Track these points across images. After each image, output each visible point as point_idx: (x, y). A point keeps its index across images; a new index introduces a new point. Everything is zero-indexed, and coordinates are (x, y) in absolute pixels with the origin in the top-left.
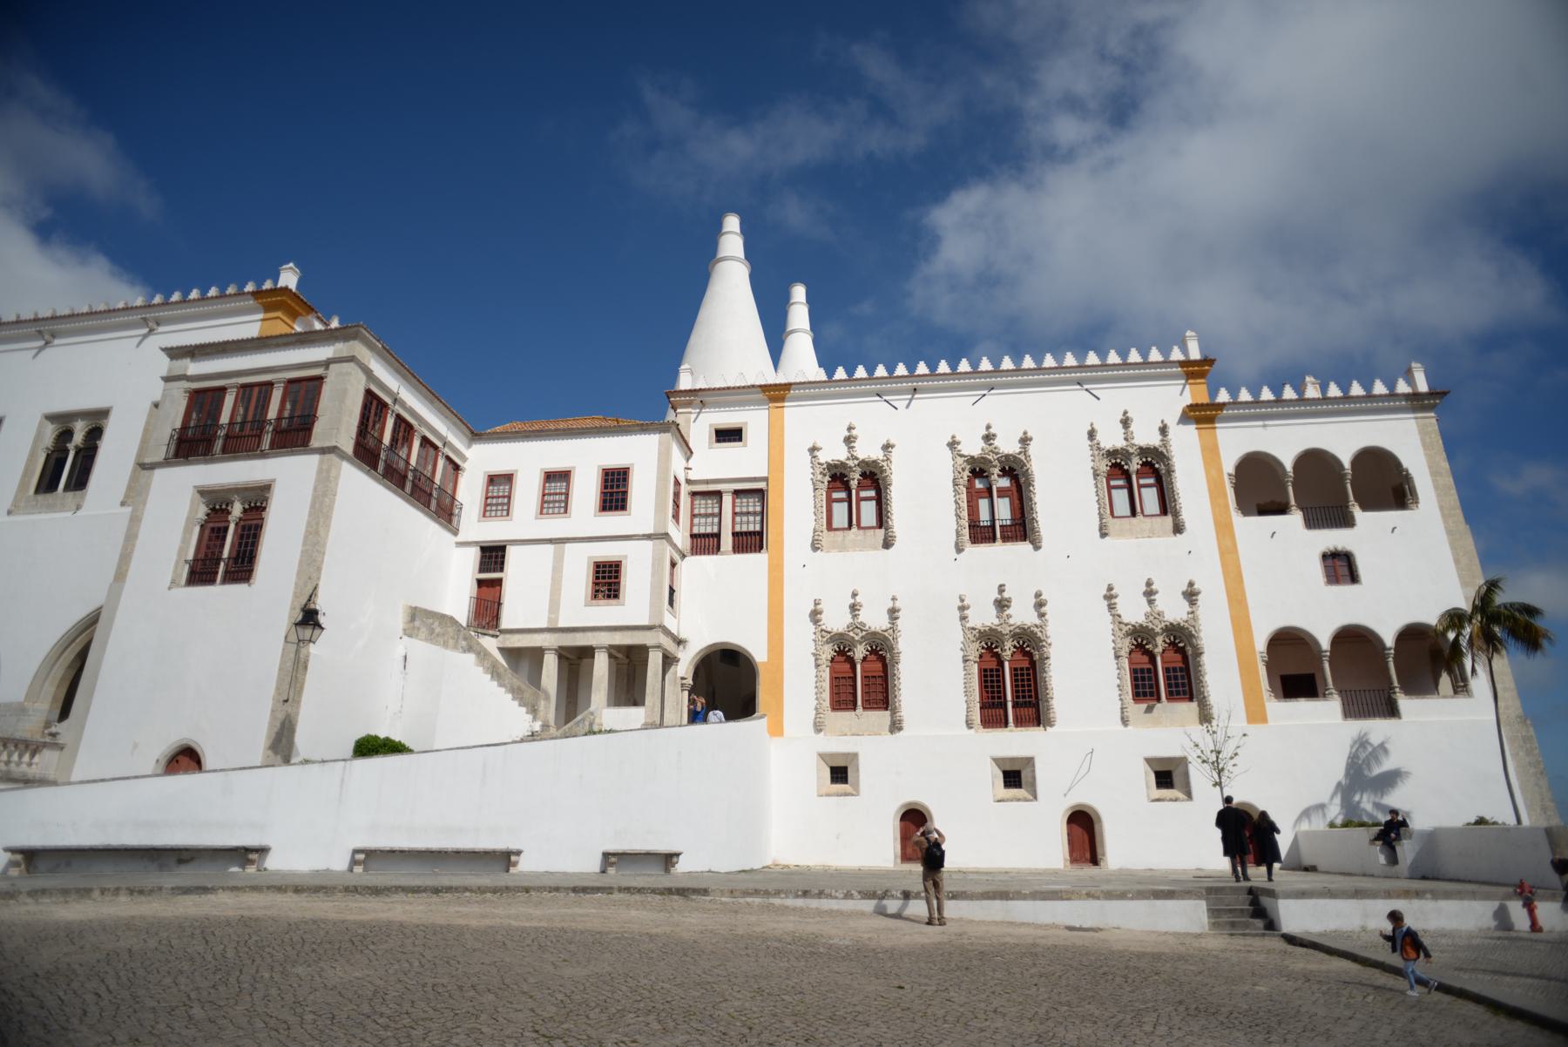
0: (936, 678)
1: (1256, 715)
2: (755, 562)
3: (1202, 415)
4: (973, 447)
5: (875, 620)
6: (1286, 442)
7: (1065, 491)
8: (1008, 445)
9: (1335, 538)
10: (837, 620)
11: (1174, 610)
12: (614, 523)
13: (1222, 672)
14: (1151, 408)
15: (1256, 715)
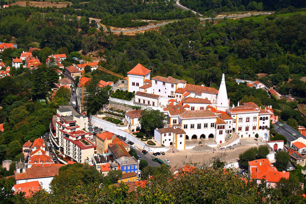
0: (244, 129)
1: (258, 130)
2: (235, 123)
3: (259, 115)
4: (247, 117)
5: (241, 126)
6: (263, 116)
7: (251, 119)
8: (249, 117)
9: (264, 121)
10: (239, 127)
11: (255, 126)
12: (230, 124)
13: (257, 128)
14: (257, 115)
15: (258, 130)
